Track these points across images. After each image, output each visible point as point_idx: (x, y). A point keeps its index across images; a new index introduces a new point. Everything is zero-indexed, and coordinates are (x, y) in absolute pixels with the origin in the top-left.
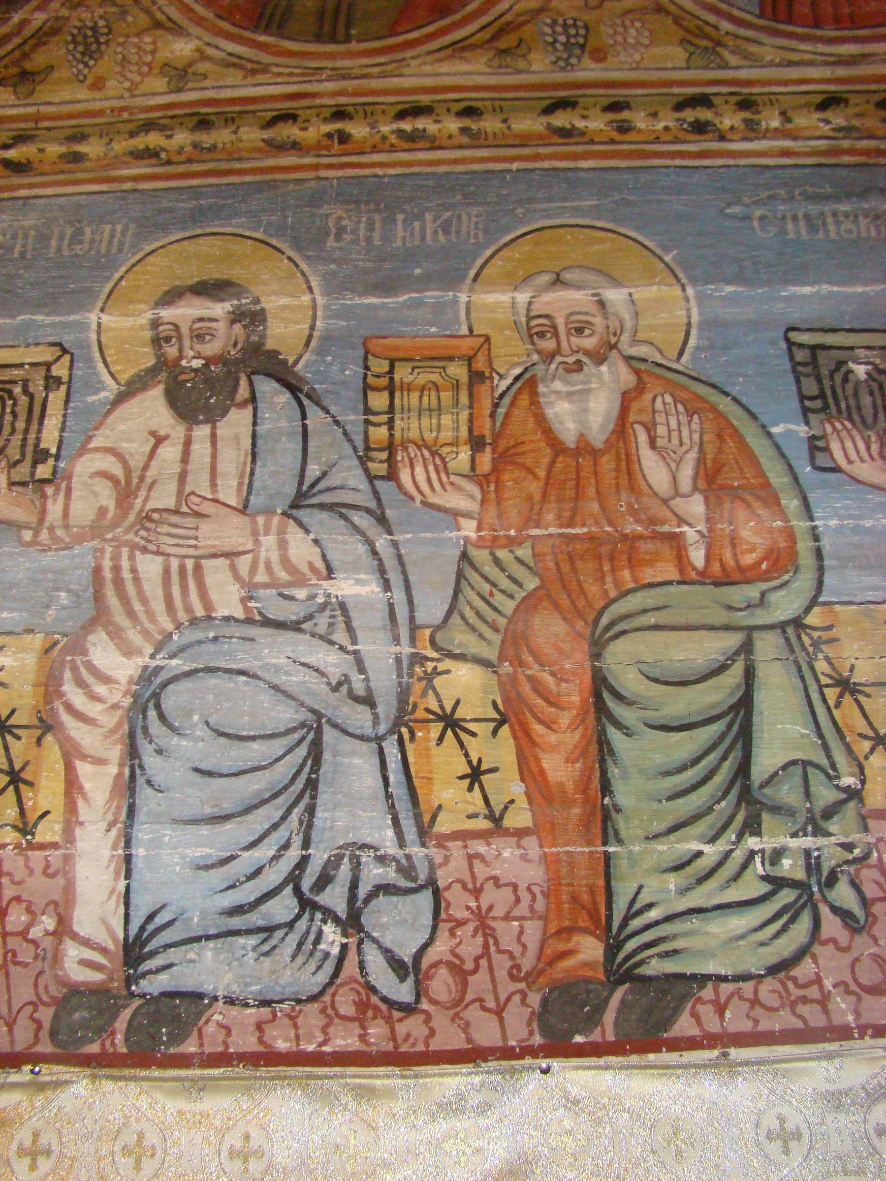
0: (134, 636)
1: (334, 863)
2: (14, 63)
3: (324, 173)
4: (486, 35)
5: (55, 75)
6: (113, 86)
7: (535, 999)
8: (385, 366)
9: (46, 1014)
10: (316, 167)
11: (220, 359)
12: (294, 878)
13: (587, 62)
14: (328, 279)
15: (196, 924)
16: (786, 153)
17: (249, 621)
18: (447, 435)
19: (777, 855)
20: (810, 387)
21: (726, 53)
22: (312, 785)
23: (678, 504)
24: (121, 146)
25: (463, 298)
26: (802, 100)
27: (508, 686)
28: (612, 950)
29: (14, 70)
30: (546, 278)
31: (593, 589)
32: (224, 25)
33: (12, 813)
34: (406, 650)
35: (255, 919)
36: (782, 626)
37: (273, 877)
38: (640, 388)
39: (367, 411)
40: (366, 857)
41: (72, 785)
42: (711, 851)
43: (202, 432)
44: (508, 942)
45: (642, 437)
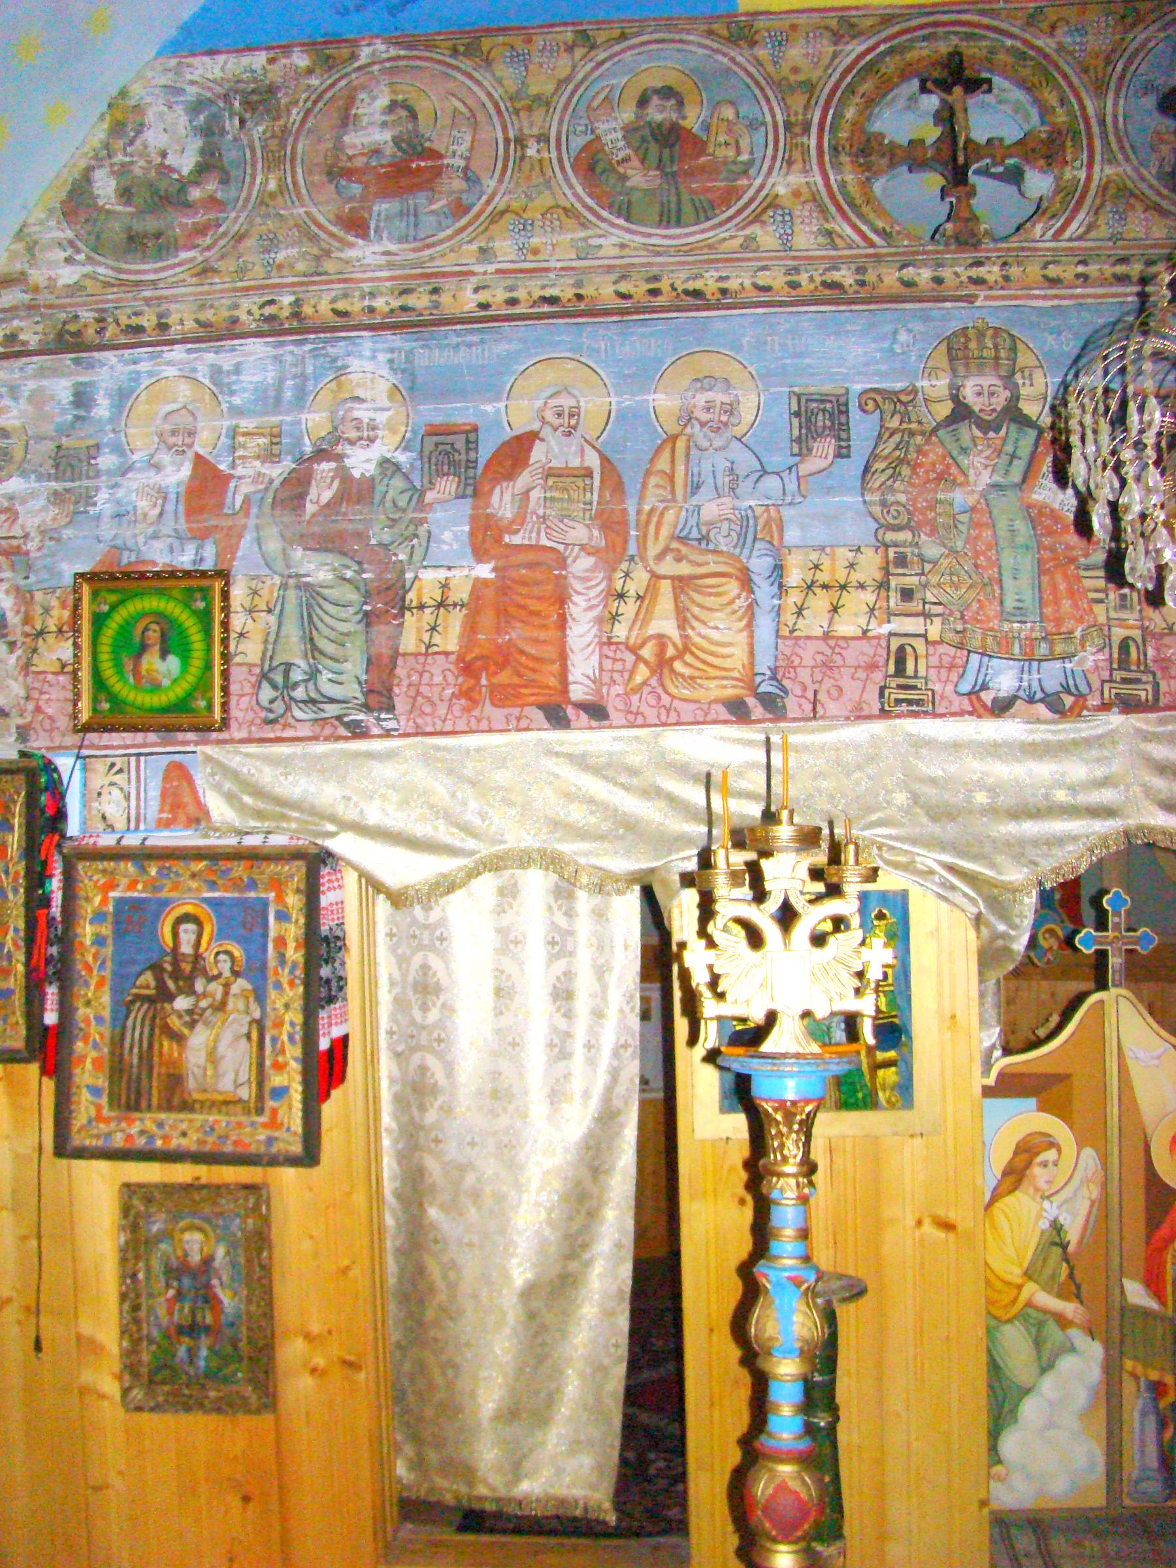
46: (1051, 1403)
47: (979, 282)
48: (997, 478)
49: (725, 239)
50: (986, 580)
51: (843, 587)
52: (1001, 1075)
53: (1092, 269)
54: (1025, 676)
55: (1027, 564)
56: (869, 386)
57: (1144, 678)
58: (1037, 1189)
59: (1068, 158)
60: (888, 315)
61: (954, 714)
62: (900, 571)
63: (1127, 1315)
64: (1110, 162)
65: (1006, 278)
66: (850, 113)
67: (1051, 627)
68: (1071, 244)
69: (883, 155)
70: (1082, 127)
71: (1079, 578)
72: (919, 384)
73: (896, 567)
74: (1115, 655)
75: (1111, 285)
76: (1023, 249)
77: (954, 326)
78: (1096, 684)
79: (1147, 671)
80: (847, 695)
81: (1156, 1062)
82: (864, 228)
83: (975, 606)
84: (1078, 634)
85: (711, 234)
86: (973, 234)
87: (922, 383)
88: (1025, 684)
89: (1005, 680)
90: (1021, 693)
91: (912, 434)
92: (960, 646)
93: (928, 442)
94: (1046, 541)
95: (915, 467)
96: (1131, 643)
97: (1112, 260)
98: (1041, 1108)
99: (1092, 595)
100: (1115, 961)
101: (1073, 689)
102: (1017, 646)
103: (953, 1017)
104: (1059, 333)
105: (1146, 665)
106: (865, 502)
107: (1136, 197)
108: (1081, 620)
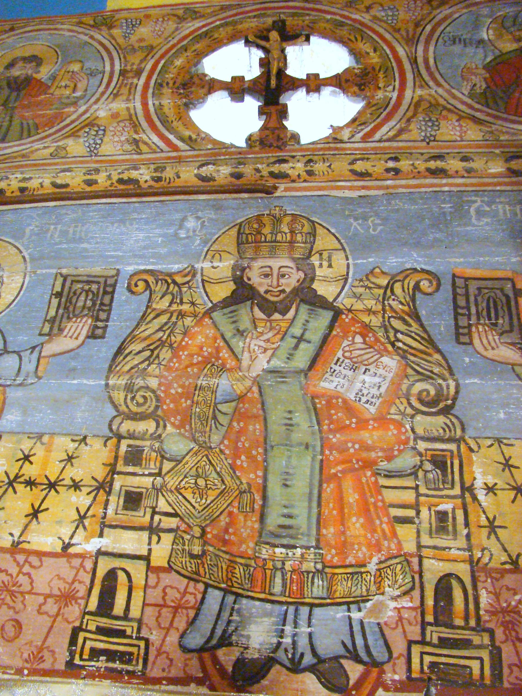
48: (276, 363)
49: (39, 149)
50: (245, 486)
51: (52, 486)
53: (404, 164)
54: (288, 629)
56: (142, 268)
57: (476, 640)
59: (381, 85)
60: (180, 206)
62: (131, 469)
64: (421, 87)
65: (310, 173)
66: (178, 62)
69: (203, 87)
70: (394, 64)
71: (379, 489)
72: (198, 266)
73: (127, 463)
74: (430, 602)
75: (425, 177)
76: (329, 149)
80: (28, 634)
82: (171, 137)
83: (224, 520)
84: (372, 567)
85: (29, 146)
86: (279, 138)
88: (287, 640)
90: (281, 655)
91: (182, 315)
94: (335, 439)
95: (176, 350)
96: (454, 583)
97: (426, 156)
99: (395, 512)
101: (362, 653)
102: (278, 580)
104: (365, 218)
105: (478, 618)
106: (107, 385)
107: (449, 110)
108: (378, 547)
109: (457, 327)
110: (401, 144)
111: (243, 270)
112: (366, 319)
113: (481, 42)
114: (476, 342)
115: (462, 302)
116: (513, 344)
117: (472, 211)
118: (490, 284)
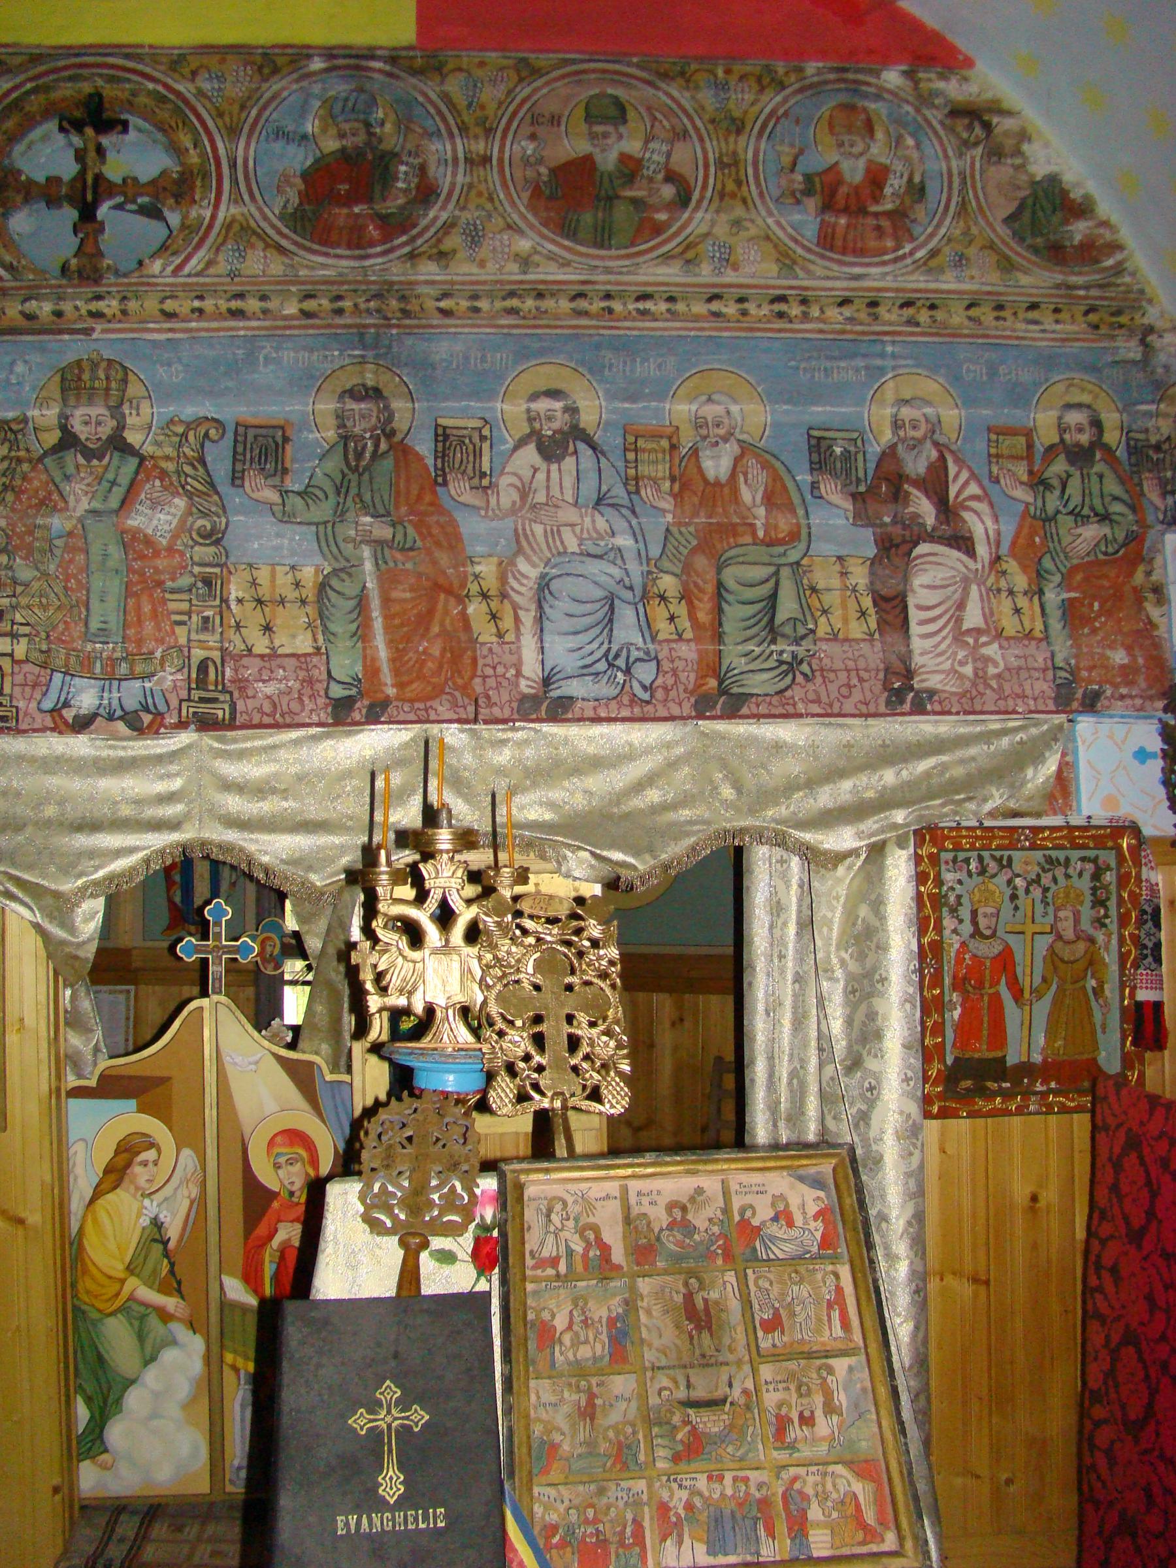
0: (535, 559)
1: (621, 649)
2: (436, 246)
3: (602, 332)
4: (679, 249)
5: (458, 256)
6: (491, 267)
7: (693, 700)
8: (632, 439)
9: (515, 705)
10: (598, 327)
11: (560, 431)
12: (606, 655)
13: (729, 271)
14: (607, 391)
15: (569, 671)
16: (821, 331)
17: (581, 554)
18: (660, 474)
19: (782, 652)
20: (815, 457)
21: (797, 270)
22: (611, 621)
23: (754, 510)
24: (499, 305)
25: (668, 406)
26: (831, 300)
27: (685, 585)
28: (721, 683)
29: (435, 251)
30: (704, 398)
31: (719, 546)
32: (545, 231)
33: (494, 630)
34: (645, 568)
35: (591, 670)
36: (791, 565)
37: (598, 655)
38: (742, 455)
39: (626, 461)
40: (632, 648)
41: (517, 619)
42: (758, 650)
43: (554, 467)
44: (683, 679)
45: (742, 479)
46: (156, 1395)
47: (97, 315)
48: (96, 505)
52: (102, 1077)
53: (208, 304)
54: (106, 695)
55: (115, 586)
57: (222, 698)
58: (137, 1188)
59: (197, 197)
61: (35, 731)
63: (226, 1311)
64: (236, 202)
65: (124, 312)
67: (132, 648)
68: (190, 280)
70: (213, 168)
71: (164, 601)
72: (29, 414)
74: (194, 675)
75: (225, 319)
76: (143, 284)
77: (71, 357)
78: (174, 703)
79: (225, 690)
81: (253, 1067)
83: (61, 627)
84: (158, 654)
86: (96, 269)
87: (33, 413)
88: (106, 702)
89: (86, 698)
90: (101, 711)
92: (44, 666)
93: (34, 469)
94: (136, 565)
95: (18, 493)
97: (229, 295)
98: (141, 1110)
100: (216, 970)
102: (98, 665)
103: (22, 1020)
104: (169, 365)
107: (258, 235)
108: (161, 641)
109: (234, 471)
110: (207, 280)
111: (67, 418)
112: (164, 464)
113: (304, 137)
114: (247, 484)
115: (240, 449)
116: (274, 487)
117: (261, 359)
118: (263, 431)
